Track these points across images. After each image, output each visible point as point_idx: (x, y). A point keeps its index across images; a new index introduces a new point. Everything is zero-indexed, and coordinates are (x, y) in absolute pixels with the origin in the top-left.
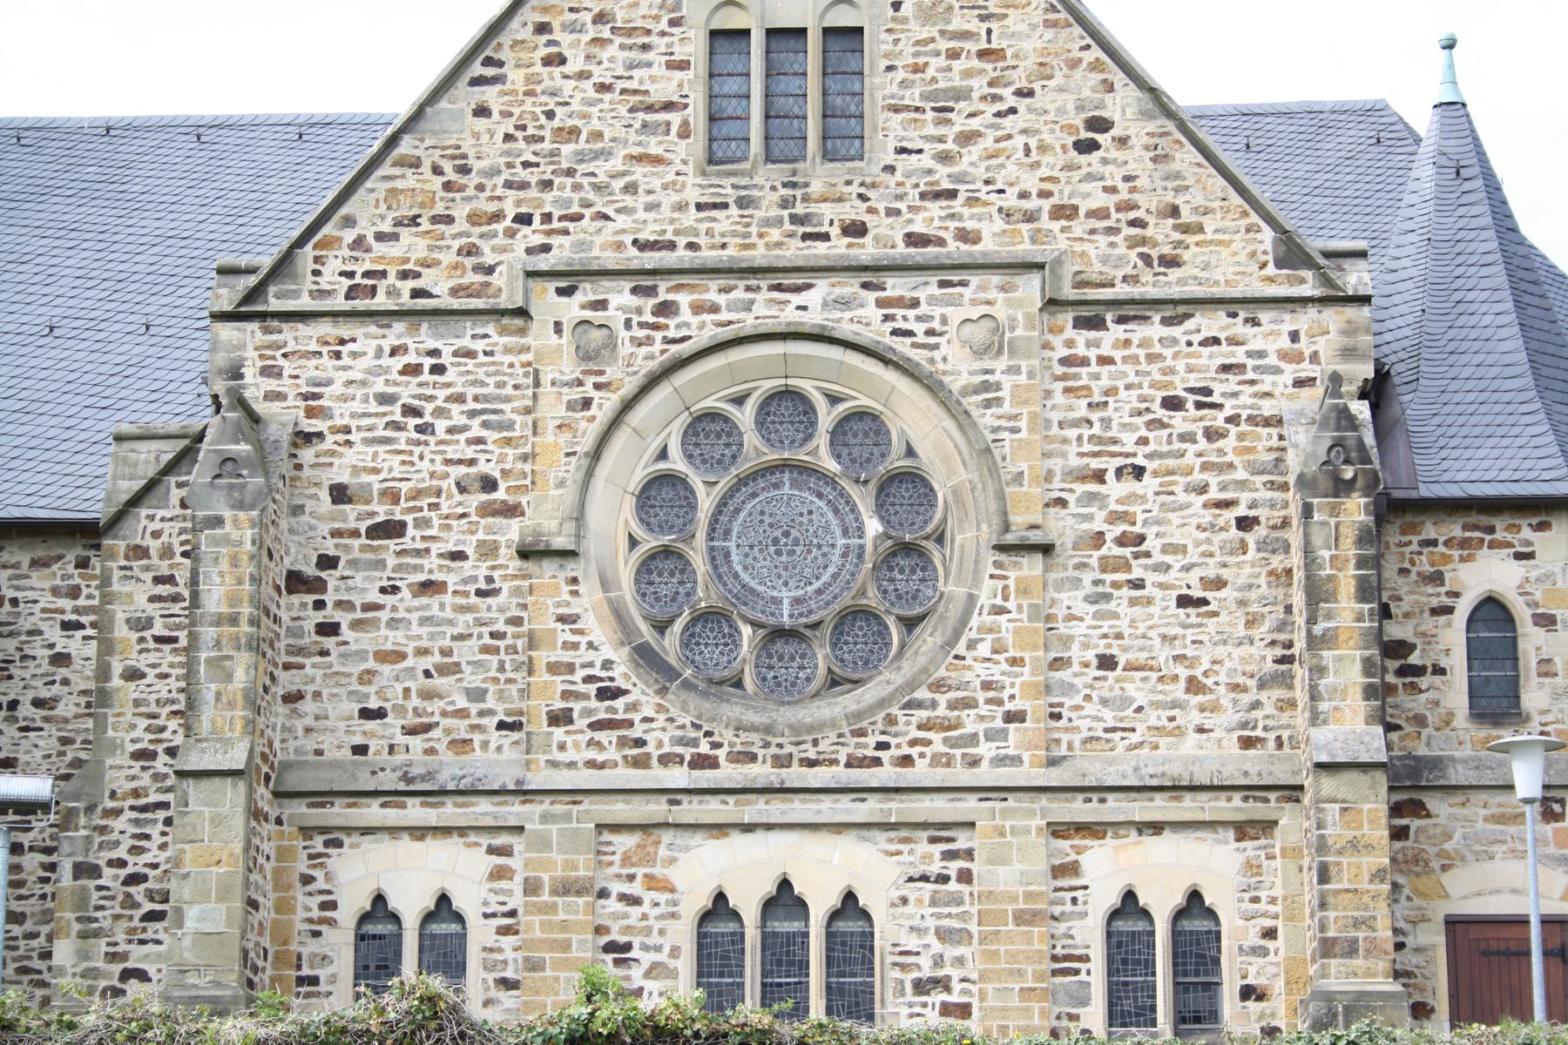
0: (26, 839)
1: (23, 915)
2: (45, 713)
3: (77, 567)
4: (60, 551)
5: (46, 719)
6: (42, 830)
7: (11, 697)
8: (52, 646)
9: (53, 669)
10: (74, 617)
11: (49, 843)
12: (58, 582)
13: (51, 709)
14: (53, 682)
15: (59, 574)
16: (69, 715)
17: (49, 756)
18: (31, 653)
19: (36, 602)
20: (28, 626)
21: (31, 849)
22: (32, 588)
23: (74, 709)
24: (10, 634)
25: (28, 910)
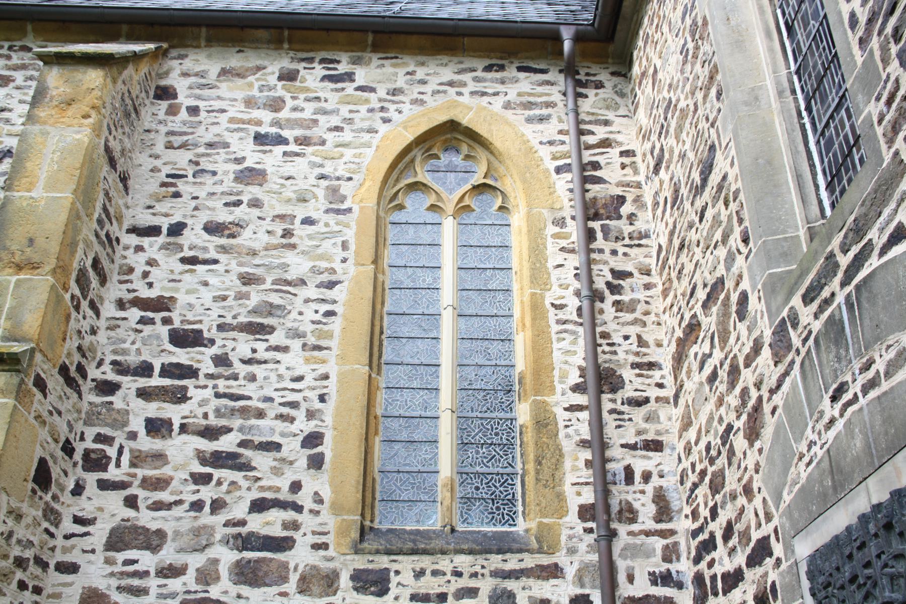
0: (175, 413)
1: (161, 534)
2: (223, 241)
3: (280, 78)
4: (259, 62)
5: (223, 249)
6: (203, 403)
7: (174, 220)
8: (239, 161)
9: (241, 187)
10: (274, 130)
11: (213, 421)
12: (255, 92)
13: (233, 236)
14: (238, 203)
15: (256, 85)
16: (257, 246)
17: (224, 298)
18: (210, 167)
19: (223, 111)
20: (209, 137)
21: (183, 428)
22: (219, 98)
23: (266, 238)
24: (183, 146)
25: (169, 528)
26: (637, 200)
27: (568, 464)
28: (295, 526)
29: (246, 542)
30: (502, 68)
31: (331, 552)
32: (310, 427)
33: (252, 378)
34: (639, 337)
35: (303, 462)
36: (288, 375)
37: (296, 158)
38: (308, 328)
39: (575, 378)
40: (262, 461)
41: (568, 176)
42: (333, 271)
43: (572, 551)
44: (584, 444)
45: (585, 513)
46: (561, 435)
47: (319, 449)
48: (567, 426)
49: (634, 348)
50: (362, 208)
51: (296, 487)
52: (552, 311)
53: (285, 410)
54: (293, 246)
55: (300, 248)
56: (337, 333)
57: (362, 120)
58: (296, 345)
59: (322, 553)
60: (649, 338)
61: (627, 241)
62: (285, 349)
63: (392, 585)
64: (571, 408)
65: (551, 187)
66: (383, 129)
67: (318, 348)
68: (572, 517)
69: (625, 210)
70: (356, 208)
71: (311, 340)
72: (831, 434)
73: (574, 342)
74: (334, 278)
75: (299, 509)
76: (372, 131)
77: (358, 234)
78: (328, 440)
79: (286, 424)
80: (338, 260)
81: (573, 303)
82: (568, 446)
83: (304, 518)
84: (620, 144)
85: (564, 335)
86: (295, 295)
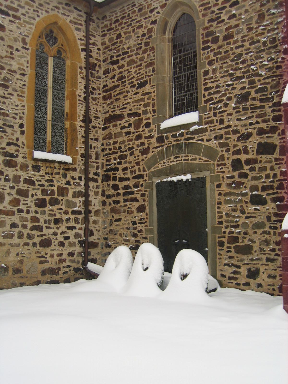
10: (6, 9)
26: (99, 66)
27: (79, 142)
28: (18, 151)
29: (6, 154)
30: (70, 6)
31: (27, 159)
32: (20, 122)
33: (4, 103)
34: (96, 109)
35: (19, 133)
36: (14, 104)
37: (13, 24)
38: (19, 89)
39: (81, 118)
40: (9, 130)
41: (84, 53)
42: (24, 70)
43: (79, 165)
44: (82, 136)
45: (82, 155)
46: (78, 134)
47: (23, 129)
48: (79, 131)
49: (95, 112)
50: (32, 49)
51: (17, 139)
52: (78, 97)
53: (14, 115)
54: (13, 58)
55: (15, 60)
56: (26, 92)
57: (32, 14)
58: (15, 94)
59: (25, 159)
60: (98, 110)
61: (96, 79)
62: (12, 95)
63: (41, 170)
64: (81, 126)
65: (80, 55)
66: (37, 19)
67: (22, 96)
68: (79, 156)
69: (97, 68)
70: (30, 49)
71: (20, 93)
72: (172, 164)
73: (82, 107)
74: (25, 73)
75: (19, 146)
76: (34, 19)
77: (31, 58)
78: (25, 126)
79: (14, 120)
80: (26, 66)
81: (83, 95)
82: (79, 137)
83: (20, 149)
84: (97, 45)
85: (80, 105)
86: (14, 76)
